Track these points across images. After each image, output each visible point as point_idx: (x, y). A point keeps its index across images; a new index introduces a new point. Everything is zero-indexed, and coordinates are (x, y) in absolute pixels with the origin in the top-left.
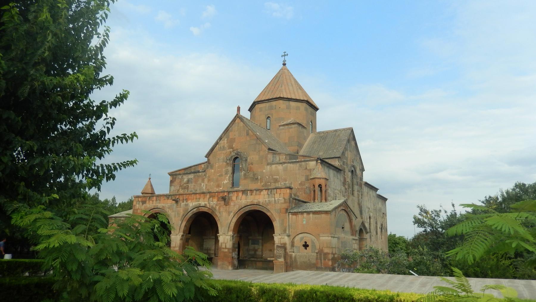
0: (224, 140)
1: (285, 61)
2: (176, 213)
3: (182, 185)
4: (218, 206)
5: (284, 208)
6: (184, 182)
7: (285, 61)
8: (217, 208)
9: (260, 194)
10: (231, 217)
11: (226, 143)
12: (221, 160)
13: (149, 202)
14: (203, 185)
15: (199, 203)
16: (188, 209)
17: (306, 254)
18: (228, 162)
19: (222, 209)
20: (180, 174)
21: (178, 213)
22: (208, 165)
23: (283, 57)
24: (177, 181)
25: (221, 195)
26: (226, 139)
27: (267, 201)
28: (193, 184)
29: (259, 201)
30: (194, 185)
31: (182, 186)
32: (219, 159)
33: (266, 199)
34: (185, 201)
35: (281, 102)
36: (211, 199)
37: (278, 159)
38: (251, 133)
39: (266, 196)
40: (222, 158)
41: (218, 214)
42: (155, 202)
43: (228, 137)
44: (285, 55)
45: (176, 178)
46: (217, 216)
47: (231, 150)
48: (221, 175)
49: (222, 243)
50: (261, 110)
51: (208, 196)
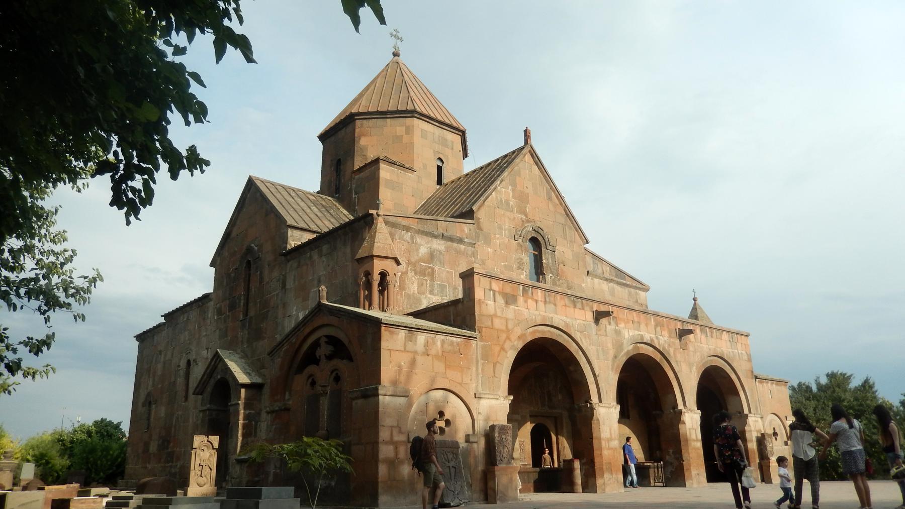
0: (508, 189)
2: (600, 348)
3: (413, 260)
4: (672, 347)
5: (749, 370)
6: (420, 255)
9: (721, 339)
10: (694, 372)
11: (511, 195)
12: (505, 230)
13: (526, 302)
15: (640, 333)
16: (622, 344)
17: (780, 447)
18: (520, 241)
19: (679, 357)
20: (407, 229)
21: (603, 349)
22: (478, 231)
25: (672, 327)
26: (510, 187)
28: (447, 269)
29: (722, 351)
30: (448, 272)
31: (414, 264)
32: (500, 228)
33: (730, 350)
34: (612, 322)
36: (658, 329)
37: (600, 271)
38: (556, 199)
39: (729, 343)
43: (514, 184)
45: (395, 234)
47: (524, 217)
49: (690, 429)
51: (653, 323)
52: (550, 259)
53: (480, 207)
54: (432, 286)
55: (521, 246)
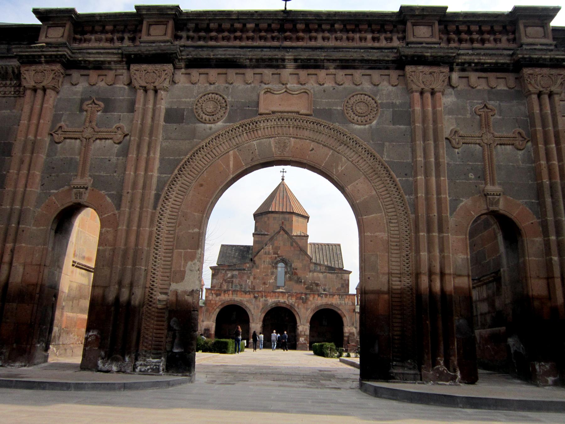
1: (283, 177)
3: (225, 279)
7: (283, 177)
8: (296, 305)
14: (249, 282)
18: (273, 265)
19: (300, 306)
20: (223, 270)
21: (257, 307)
23: (282, 173)
24: (220, 275)
25: (299, 296)
26: (271, 246)
27: (339, 303)
28: (238, 279)
32: (264, 262)
35: (294, 215)
36: (290, 298)
40: (267, 261)
41: (296, 309)
42: (231, 295)
43: (273, 245)
44: (283, 172)
46: (295, 311)
47: (276, 255)
48: (267, 275)
49: (301, 332)
50: (275, 219)
51: (287, 295)
52: (289, 269)
53: (255, 256)
54: (232, 286)
55: (274, 267)
